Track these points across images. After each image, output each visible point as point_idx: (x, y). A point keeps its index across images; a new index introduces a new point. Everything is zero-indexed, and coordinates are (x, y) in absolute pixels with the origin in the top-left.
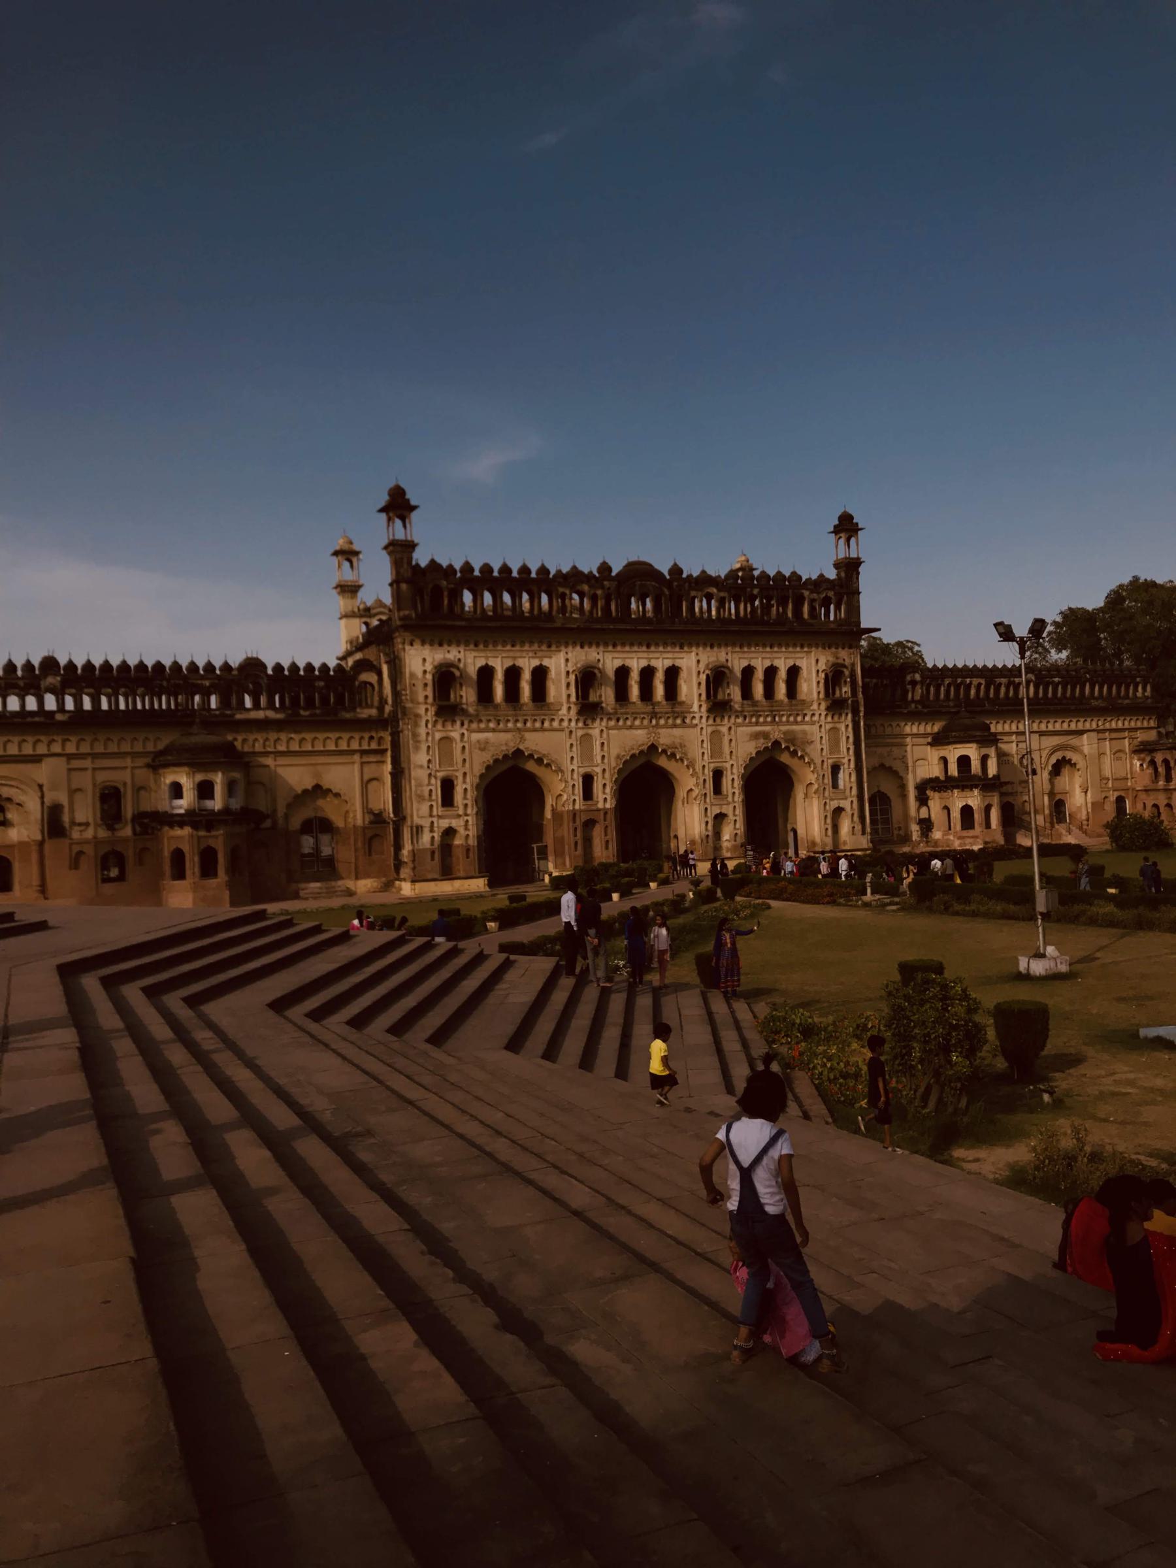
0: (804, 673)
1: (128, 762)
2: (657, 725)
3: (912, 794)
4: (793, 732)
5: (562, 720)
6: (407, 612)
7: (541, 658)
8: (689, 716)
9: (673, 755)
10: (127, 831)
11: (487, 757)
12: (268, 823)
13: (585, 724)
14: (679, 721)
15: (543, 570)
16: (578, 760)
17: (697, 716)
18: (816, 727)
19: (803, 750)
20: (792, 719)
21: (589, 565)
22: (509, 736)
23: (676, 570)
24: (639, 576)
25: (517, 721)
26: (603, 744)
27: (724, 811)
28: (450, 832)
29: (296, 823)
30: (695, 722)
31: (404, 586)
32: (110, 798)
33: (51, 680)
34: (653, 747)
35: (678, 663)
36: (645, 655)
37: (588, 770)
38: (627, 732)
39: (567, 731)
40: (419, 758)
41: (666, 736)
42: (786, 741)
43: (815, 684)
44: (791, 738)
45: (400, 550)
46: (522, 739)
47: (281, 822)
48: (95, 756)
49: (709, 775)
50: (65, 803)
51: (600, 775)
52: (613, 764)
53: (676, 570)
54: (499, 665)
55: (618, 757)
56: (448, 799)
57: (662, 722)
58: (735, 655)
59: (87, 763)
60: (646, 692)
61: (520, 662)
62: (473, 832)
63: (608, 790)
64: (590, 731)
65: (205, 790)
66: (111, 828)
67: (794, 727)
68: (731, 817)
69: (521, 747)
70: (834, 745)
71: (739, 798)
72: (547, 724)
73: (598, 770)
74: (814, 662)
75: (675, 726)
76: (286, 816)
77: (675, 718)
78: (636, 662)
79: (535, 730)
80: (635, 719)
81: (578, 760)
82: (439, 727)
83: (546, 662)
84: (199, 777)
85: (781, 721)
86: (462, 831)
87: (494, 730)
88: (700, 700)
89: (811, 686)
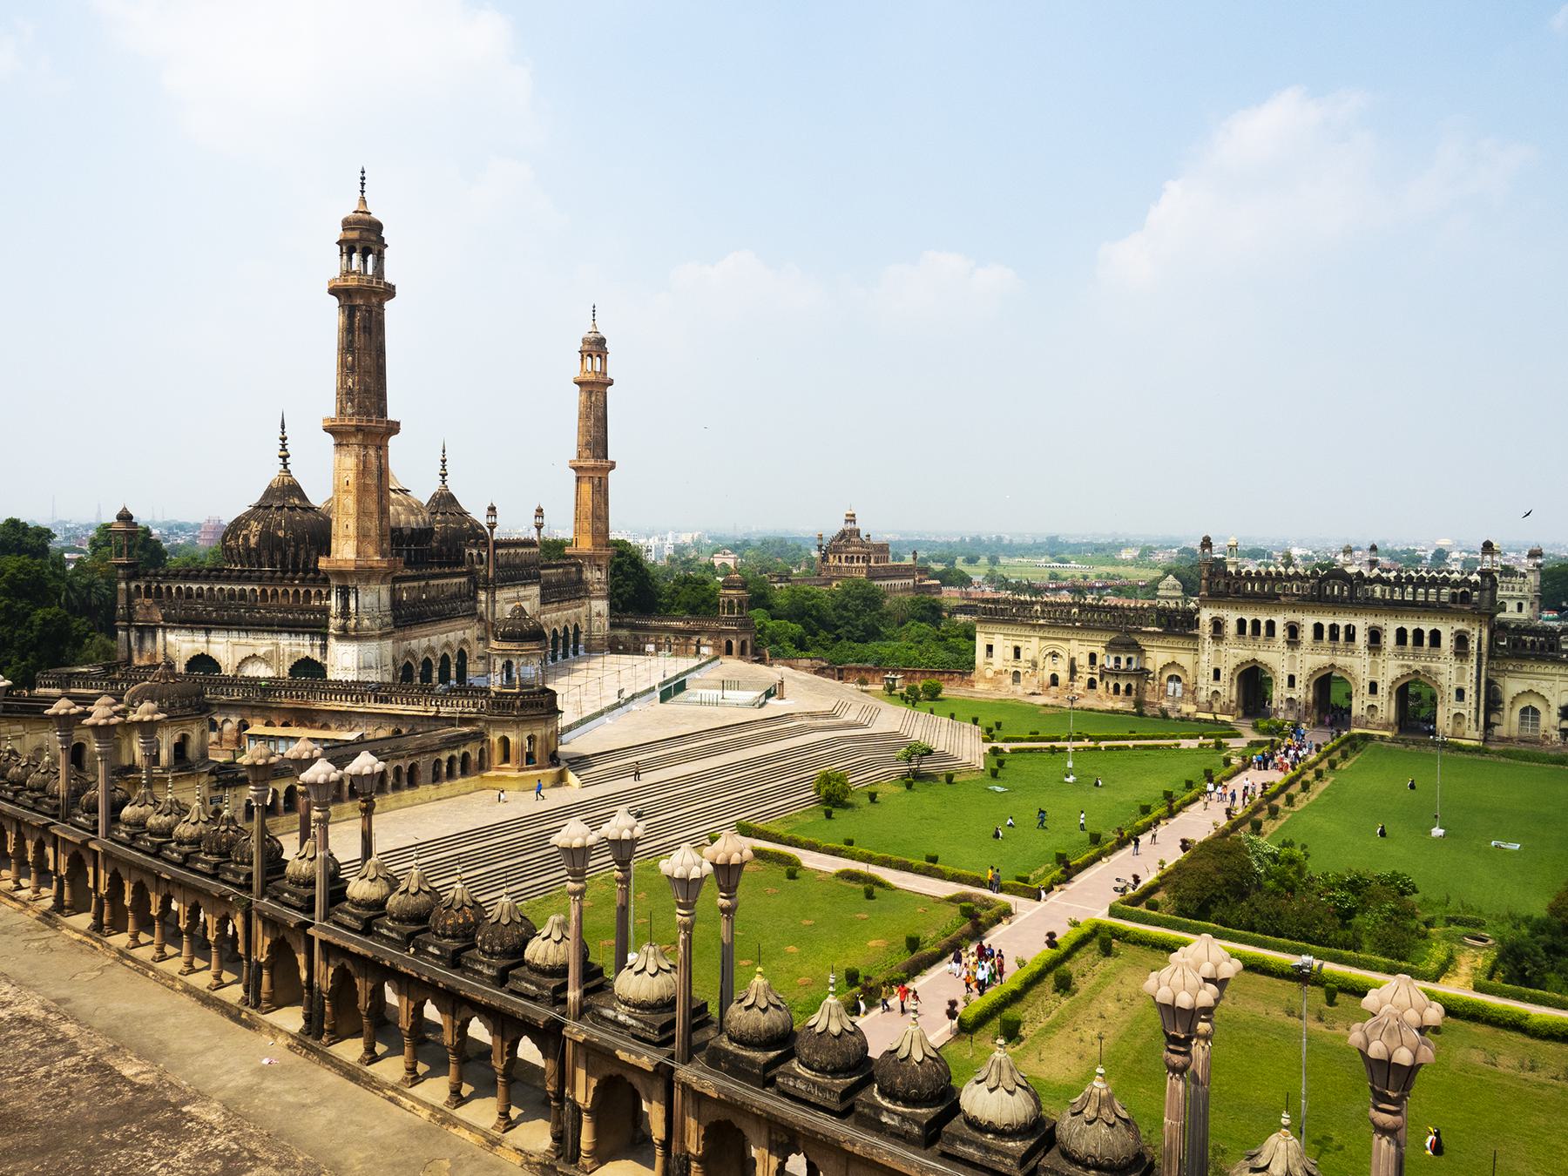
3: (1555, 711)
16: (1292, 668)
28: (1216, 692)
29: (1166, 675)
32: (1093, 657)
33: (1075, 610)
34: (1332, 665)
40: (1204, 658)
41: (1341, 660)
44: (1428, 670)
52: (1306, 672)
54: (1249, 618)
60: (1334, 636)
65: (1118, 660)
70: (1461, 676)
71: (1386, 698)
78: (1326, 621)
81: (1292, 668)
89: (1447, 642)
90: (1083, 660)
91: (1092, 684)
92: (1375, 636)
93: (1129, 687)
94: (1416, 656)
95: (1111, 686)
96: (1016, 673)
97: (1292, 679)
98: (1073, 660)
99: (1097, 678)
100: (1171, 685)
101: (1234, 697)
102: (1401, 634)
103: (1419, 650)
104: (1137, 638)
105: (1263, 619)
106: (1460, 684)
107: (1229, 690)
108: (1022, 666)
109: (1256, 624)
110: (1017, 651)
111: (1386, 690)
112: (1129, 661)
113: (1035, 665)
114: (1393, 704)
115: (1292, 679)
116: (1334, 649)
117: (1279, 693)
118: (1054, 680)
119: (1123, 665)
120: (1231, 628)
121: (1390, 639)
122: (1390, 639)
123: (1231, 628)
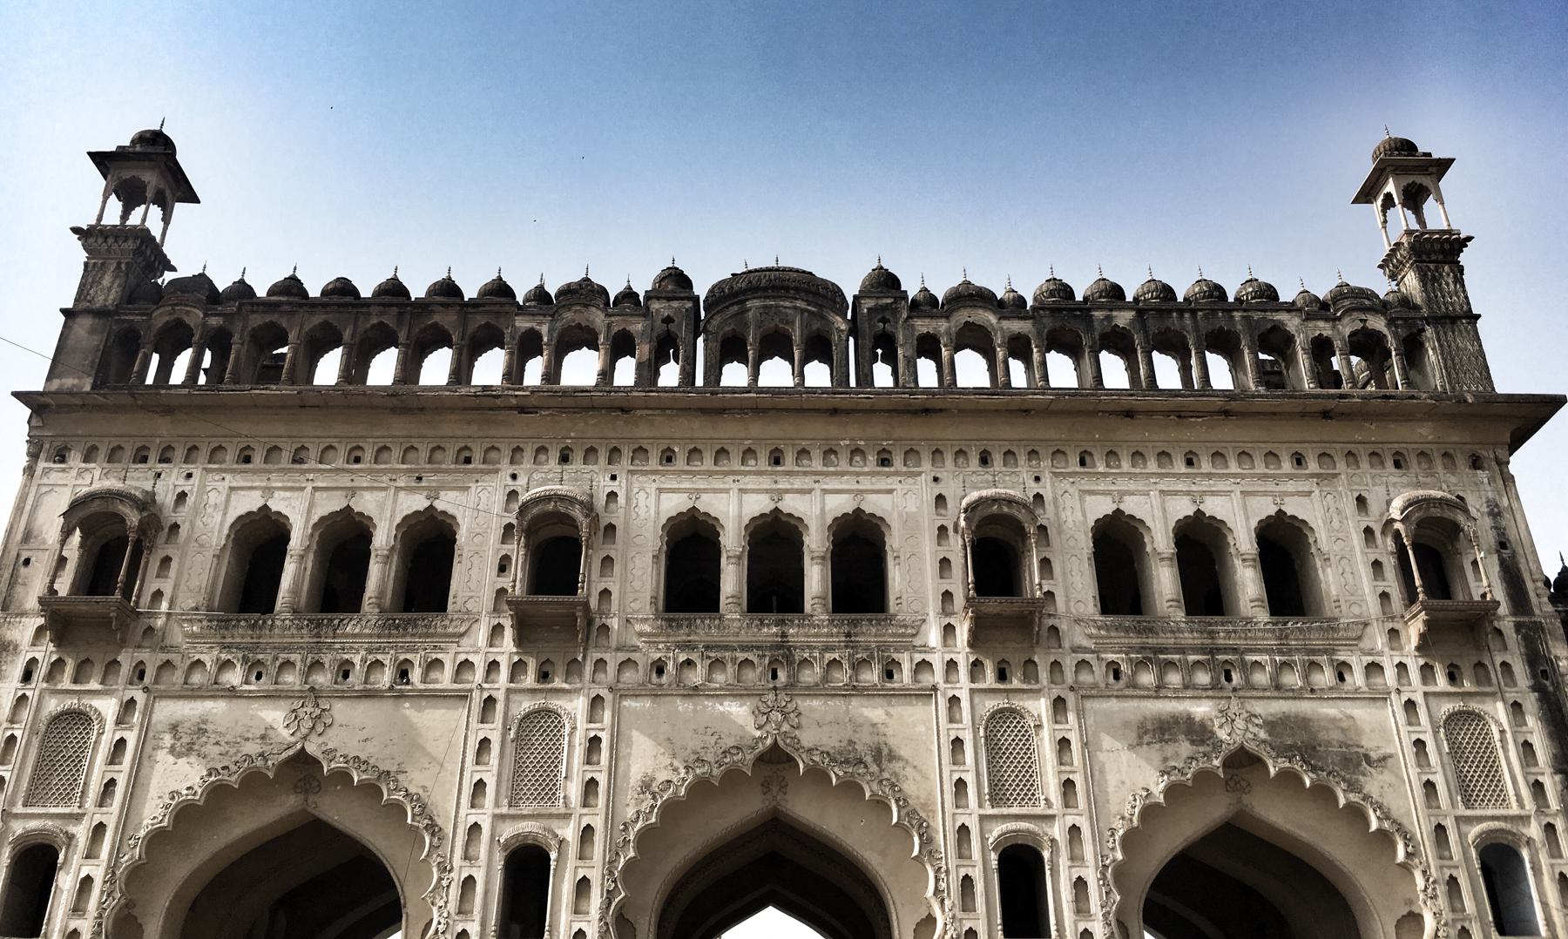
2: (792, 685)
4: (1303, 723)
5: (466, 665)
6: (69, 382)
7: (433, 494)
9: (851, 788)
13: (544, 676)
14: (872, 676)
18: (1393, 713)
19: (1353, 787)
20: (1293, 679)
25: (317, 665)
26: (594, 742)
30: (926, 680)
31: (84, 324)
34: (775, 760)
35: (874, 505)
36: (766, 482)
38: (683, 706)
39: (477, 700)
41: (821, 724)
42: (1283, 751)
43: (1365, 572)
46: (320, 722)
49: (982, 867)
51: (573, 849)
55: (646, 786)
57: (809, 676)
58: (1065, 484)
60: (775, 590)
61: (366, 504)
63: (596, 900)
64: (556, 703)
67: (1305, 707)
69: (312, 748)
72: (416, 675)
74: (1350, 506)
75: (855, 690)
77: (857, 666)
78: (734, 504)
79: (370, 695)
80: (717, 664)
82: (66, 683)
83: (447, 502)
85: (1250, 686)
87: (232, 693)
88: (945, 612)
94: (1225, 671)
102: (1117, 546)
105: (388, 509)
106: (1486, 819)
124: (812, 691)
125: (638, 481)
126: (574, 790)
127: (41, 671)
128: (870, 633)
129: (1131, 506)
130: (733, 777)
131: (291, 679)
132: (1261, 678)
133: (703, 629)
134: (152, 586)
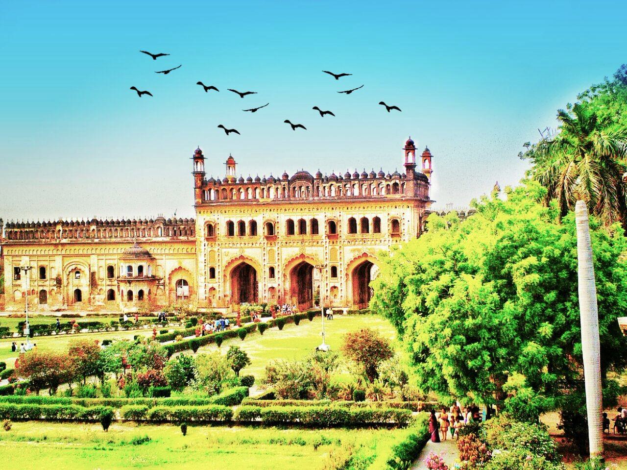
0: (382, 222)
1: (116, 257)
8: (320, 241)
10: (116, 283)
11: (228, 259)
12: (162, 282)
15: (258, 179)
17: (324, 241)
21: (279, 175)
22: (238, 250)
23: (320, 175)
24: (302, 176)
27: (336, 285)
28: (213, 289)
31: (197, 190)
32: (111, 270)
33: (93, 227)
34: (302, 256)
36: (300, 214)
37: (272, 265)
40: (201, 258)
41: (309, 251)
45: (200, 175)
47: (167, 281)
48: (106, 255)
50: (96, 271)
53: (320, 175)
55: (286, 259)
56: (213, 275)
57: (307, 244)
59: (103, 257)
62: (221, 289)
64: (273, 248)
65: (130, 268)
66: (111, 281)
68: (340, 289)
69: (243, 255)
72: (254, 245)
73: (276, 265)
76: (170, 279)
79: (248, 248)
83: (255, 219)
84: (128, 265)
86: (217, 288)
90: (103, 273)
91: (111, 296)
92: (332, 226)
93: (141, 293)
94: (364, 241)
95: (125, 293)
96: (43, 293)
97: (272, 270)
98: (93, 275)
99: (115, 289)
100: (179, 289)
101: (228, 292)
103: (366, 235)
104: (147, 248)
107: (225, 286)
108: (49, 285)
109: (242, 224)
110: (43, 271)
111: (344, 273)
112: (141, 269)
113: (59, 281)
114: (350, 283)
115: (272, 270)
116: (303, 241)
117: (263, 283)
118: (78, 293)
119: (135, 272)
120: (222, 230)
121: (343, 228)
122: (343, 228)
123: (222, 230)
124: (307, 246)
125: (282, 214)
126: (277, 260)
127: (206, 245)
128: (315, 237)
129: (354, 216)
130: (297, 258)
131: (238, 245)
132: (369, 242)
133: (292, 237)
134: (217, 232)
